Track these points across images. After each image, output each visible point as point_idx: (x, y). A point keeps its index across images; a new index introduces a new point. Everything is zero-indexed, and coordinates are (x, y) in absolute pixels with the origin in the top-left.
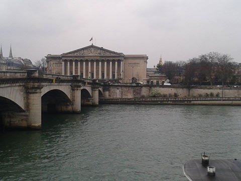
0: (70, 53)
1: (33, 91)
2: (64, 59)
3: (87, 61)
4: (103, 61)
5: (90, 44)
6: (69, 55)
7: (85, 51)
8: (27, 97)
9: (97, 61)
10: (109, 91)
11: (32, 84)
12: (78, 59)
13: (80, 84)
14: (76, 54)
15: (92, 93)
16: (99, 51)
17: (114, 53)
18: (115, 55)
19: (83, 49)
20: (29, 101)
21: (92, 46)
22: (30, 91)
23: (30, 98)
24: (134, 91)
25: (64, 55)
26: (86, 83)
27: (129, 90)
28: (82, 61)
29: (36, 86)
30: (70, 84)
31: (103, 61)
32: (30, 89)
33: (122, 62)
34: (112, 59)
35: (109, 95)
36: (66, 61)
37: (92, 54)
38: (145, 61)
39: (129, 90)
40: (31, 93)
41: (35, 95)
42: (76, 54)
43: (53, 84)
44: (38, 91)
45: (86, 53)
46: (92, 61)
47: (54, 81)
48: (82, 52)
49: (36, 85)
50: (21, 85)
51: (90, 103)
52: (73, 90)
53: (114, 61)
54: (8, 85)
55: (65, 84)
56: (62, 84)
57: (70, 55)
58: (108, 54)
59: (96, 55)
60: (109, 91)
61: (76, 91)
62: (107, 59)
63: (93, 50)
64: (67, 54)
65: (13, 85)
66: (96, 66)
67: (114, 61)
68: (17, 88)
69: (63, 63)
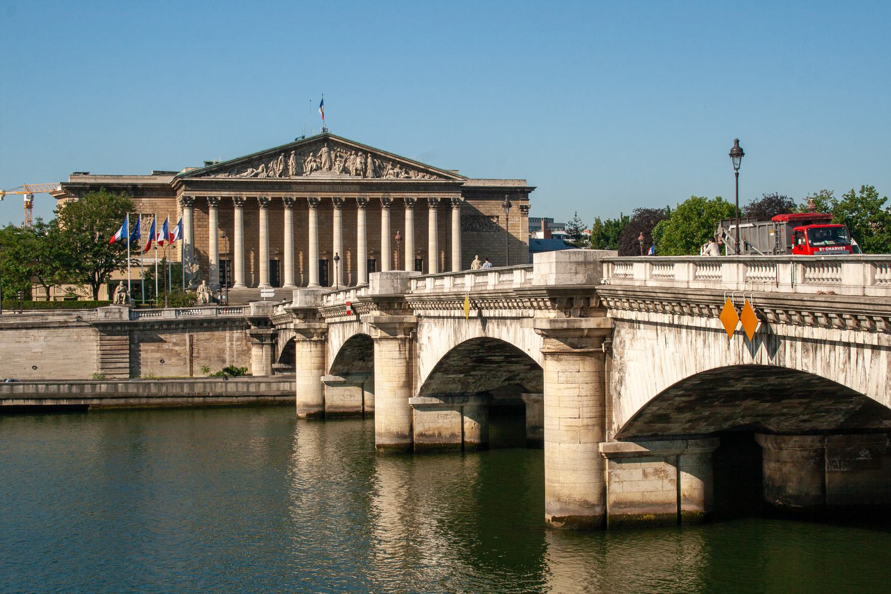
2: (194, 195)
5: (314, 131)
6: (212, 178)
14: (247, 175)
17: (426, 170)
18: (427, 179)
19: (285, 151)
21: (325, 140)
34: (415, 196)
37: (322, 171)
38: (522, 208)
42: (247, 175)
57: (221, 177)
59: (346, 177)
64: (208, 172)
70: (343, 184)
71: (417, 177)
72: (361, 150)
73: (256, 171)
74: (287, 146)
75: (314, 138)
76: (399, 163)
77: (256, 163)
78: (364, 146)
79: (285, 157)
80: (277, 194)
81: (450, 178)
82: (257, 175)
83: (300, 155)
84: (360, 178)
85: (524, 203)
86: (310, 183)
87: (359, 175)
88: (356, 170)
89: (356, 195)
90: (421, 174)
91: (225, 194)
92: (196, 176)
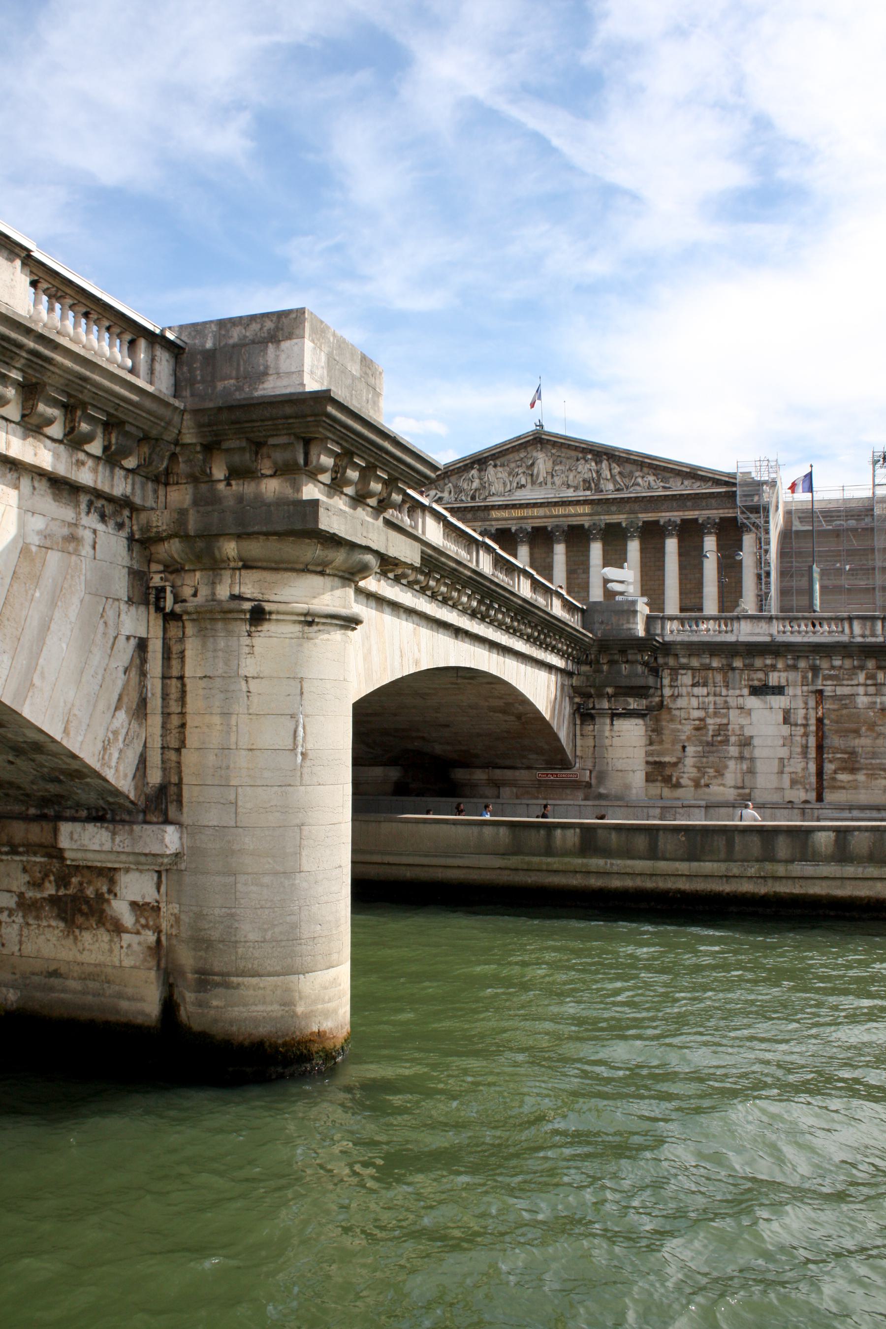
9: (578, 538)
10: (655, 714)
15: (159, 691)
16: (587, 468)
17: (693, 474)
21: (538, 440)
34: (676, 516)
35: (659, 772)
48: (473, 481)
51: (111, 967)
53: (690, 533)
58: (647, 485)
59: (570, 494)
60: (655, 714)
63: (543, 462)
67: (690, 533)
71: (679, 488)
72: (591, 451)
73: (440, 495)
74: (481, 453)
76: (650, 466)
77: (441, 483)
78: (593, 444)
79: (480, 470)
83: (502, 465)
84: (588, 493)
86: (514, 506)
87: (589, 488)
88: (584, 481)
89: (586, 522)
90: (686, 482)
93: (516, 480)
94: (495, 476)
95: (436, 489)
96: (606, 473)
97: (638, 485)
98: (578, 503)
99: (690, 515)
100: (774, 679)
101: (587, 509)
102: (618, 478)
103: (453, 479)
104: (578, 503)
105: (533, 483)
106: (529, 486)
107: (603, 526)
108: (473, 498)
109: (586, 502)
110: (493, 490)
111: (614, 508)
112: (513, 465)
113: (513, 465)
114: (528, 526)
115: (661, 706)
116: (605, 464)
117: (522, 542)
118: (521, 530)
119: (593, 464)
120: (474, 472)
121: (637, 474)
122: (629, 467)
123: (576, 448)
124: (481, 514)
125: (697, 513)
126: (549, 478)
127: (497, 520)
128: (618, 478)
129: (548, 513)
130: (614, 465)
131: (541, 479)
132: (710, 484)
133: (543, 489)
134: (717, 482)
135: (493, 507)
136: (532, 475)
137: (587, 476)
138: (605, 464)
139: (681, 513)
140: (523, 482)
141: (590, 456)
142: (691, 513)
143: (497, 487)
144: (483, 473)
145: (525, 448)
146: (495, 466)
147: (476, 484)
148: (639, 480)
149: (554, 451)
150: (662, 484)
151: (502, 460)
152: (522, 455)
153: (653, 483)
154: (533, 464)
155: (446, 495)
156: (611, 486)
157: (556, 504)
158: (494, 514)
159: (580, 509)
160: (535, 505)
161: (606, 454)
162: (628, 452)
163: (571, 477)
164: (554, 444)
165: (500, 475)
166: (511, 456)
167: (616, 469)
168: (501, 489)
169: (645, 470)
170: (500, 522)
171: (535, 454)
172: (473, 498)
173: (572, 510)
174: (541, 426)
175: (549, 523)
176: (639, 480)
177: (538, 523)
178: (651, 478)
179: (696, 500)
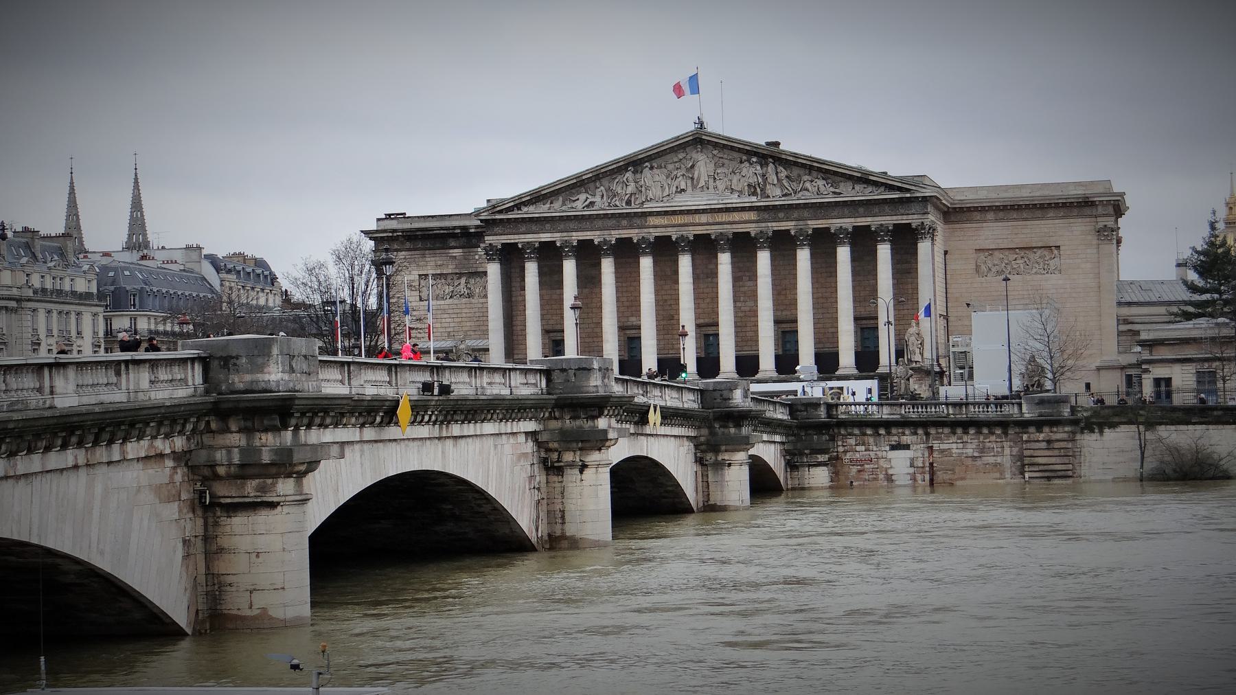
0: (537, 197)
1: (250, 489)
2: (495, 240)
3: (665, 250)
4: (783, 245)
7: (647, 176)
8: (207, 539)
9: (743, 246)
11: (236, 439)
12: (596, 236)
13: (602, 423)
14: (579, 205)
16: (751, 172)
17: (863, 178)
19: (635, 163)
20: (221, 566)
21: (699, 140)
22: (226, 492)
23: (224, 542)
24: (1022, 464)
25: (498, 217)
26: (654, 417)
27: (983, 450)
28: (626, 253)
29: (266, 458)
30: (531, 426)
31: (783, 245)
32: (230, 477)
33: (924, 247)
34: (848, 223)
36: (511, 257)
39: (983, 450)
40: (234, 508)
41: (263, 518)
42: (579, 205)
43: (392, 432)
44: (285, 487)
45: (656, 190)
46: (704, 247)
47: (404, 412)
48: (627, 185)
49: (268, 443)
50: (161, 456)
52: (552, 468)
53: (863, 242)
54: (70, 457)
55: (489, 428)
56: (469, 429)
58: (816, 191)
59: (734, 200)
60: (834, 463)
61: (572, 475)
62: (814, 224)
63: (704, 164)
65: (101, 454)
66: (736, 279)
67: (863, 242)
68: (134, 476)
69: (494, 270)
70: (728, 210)
71: (850, 193)
72: (756, 154)
74: (636, 154)
75: (677, 139)
76: (820, 170)
77: (591, 185)
79: (635, 172)
80: (625, 233)
81: (908, 190)
82: (592, 203)
83: (660, 167)
84: (754, 199)
85: (1110, 222)
86: (674, 213)
87: (754, 194)
89: (753, 229)
90: (857, 187)
91: (545, 237)
92: (500, 212)
93: (676, 183)
94: (653, 179)
95: (586, 192)
96: (772, 178)
97: (807, 190)
98: (743, 209)
99: (862, 221)
100: (907, 439)
101: (752, 216)
102: (785, 183)
103: (605, 181)
104: (743, 209)
105: (694, 187)
106: (690, 189)
107: (770, 234)
108: (628, 203)
109: (751, 209)
110: (650, 195)
111: (781, 215)
112: (670, 167)
113: (670, 167)
114: (690, 232)
115: (837, 458)
116: (771, 167)
117: (683, 251)
118: (682, 238)
119: (759, 168)
120: (629, 175)
121: (806, 178)
122: (796, 172)
123: (740, 150)
124: (638, 221)
125: (869, 219)
126: (711, 181)
127: (656, 227)
128: (785, 183)
129: (711, 221)
130: (781, 168)
131: (702, 183)
132: (882, 189)
133: (706, 194)
134: (891, 188)
135: (651, 214)
136: (692, 179)
137: (753, 180)
138: (771, 167)
139: (852, 220)
140: (683, 186)
141: (754, 160)
142: (863, 219)
143: (655, 192)
144: (638, 176)
145: (684, 148)
146: (652, 168)
147: (631, 188)
148: (808, 185)
149: (715, 152)
150: (832, 189)
151: (659, 161)
152: (681, 156)
153: (822, 189)
154: (693, 166)
155: (597, 199)
156: (778, 192)
157: (720, 210)
158: (653, 221)
159: (746, 216)
160: (697, 212)
161: (771, 157)
162: (795, 155)
163: (735, 181)
164: (716, 145)
165: (657, 178)
166: (668, 157)
167: (783, 173)
168: (659, 193)
169: (814, 173)
170: (659, 230)
171: (695, 155)
172: (628, 203)
173: (736, 216)
174: (702, 124)
175: (713, 230)
176: (808, 185)
177: (700, 230)
178: (821, 183)
179: (868, 206)
